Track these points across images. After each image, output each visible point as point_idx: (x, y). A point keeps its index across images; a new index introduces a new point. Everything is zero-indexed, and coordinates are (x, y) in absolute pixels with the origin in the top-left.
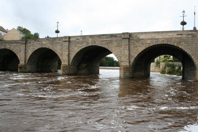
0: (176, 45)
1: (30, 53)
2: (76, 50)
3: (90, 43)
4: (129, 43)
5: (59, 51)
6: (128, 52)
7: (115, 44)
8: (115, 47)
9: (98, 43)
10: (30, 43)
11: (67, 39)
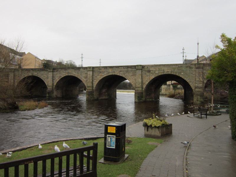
0: (177, 75)
1: (57, 79)
2: (99, 77)
3: (111, 73)
4: (142, 73)
5: (84, 79)
6: (141, 80)
7: (131, 74)
8: (131, 76)
9: (117, 73)
10: (57, 71)
11: (91, 69)
